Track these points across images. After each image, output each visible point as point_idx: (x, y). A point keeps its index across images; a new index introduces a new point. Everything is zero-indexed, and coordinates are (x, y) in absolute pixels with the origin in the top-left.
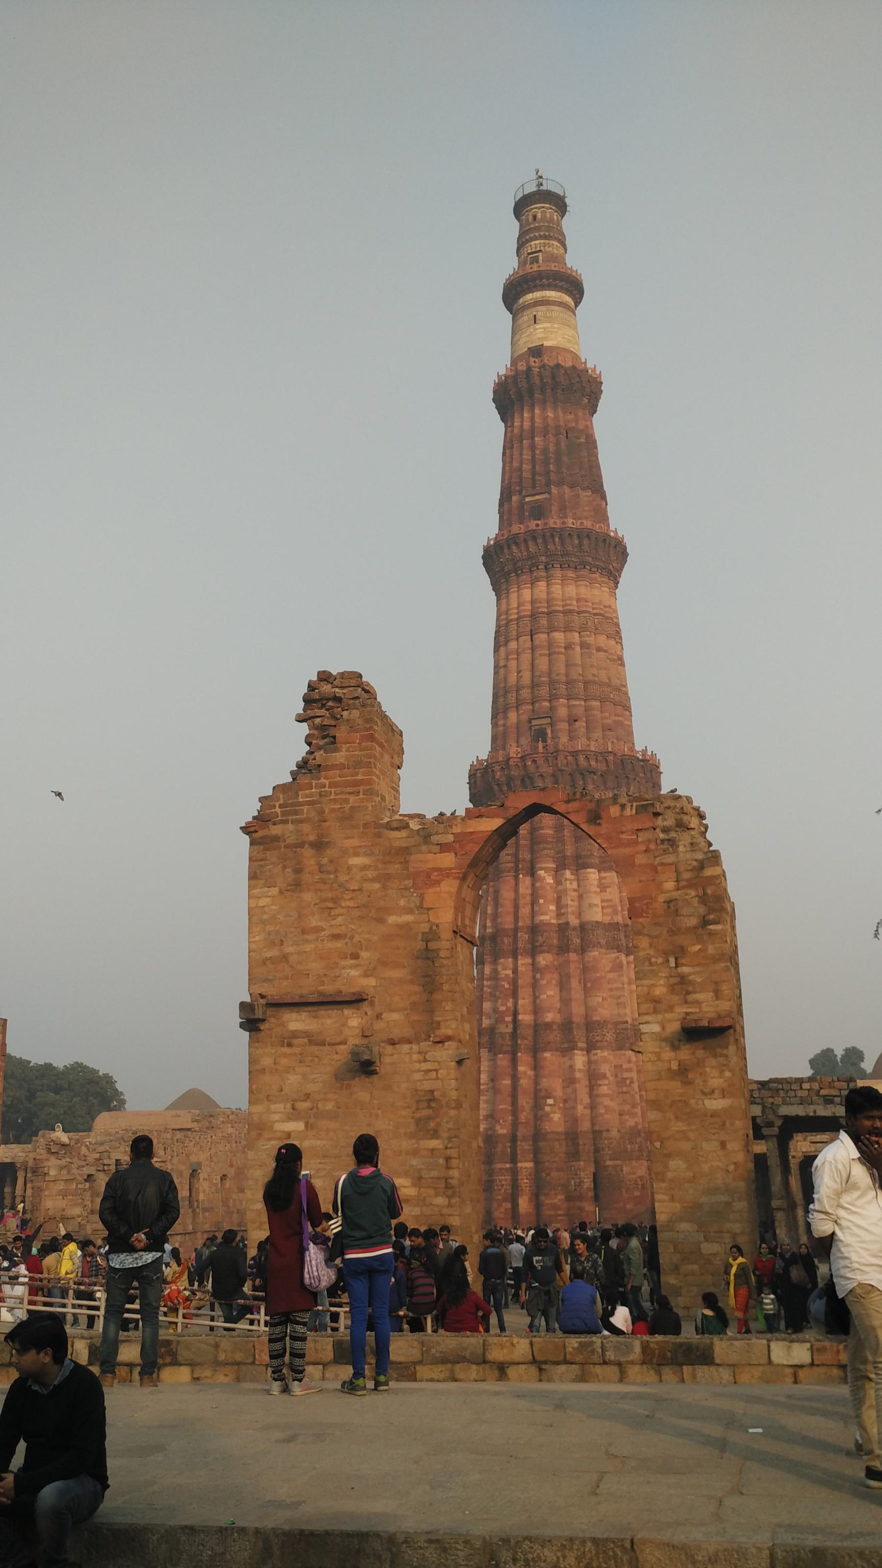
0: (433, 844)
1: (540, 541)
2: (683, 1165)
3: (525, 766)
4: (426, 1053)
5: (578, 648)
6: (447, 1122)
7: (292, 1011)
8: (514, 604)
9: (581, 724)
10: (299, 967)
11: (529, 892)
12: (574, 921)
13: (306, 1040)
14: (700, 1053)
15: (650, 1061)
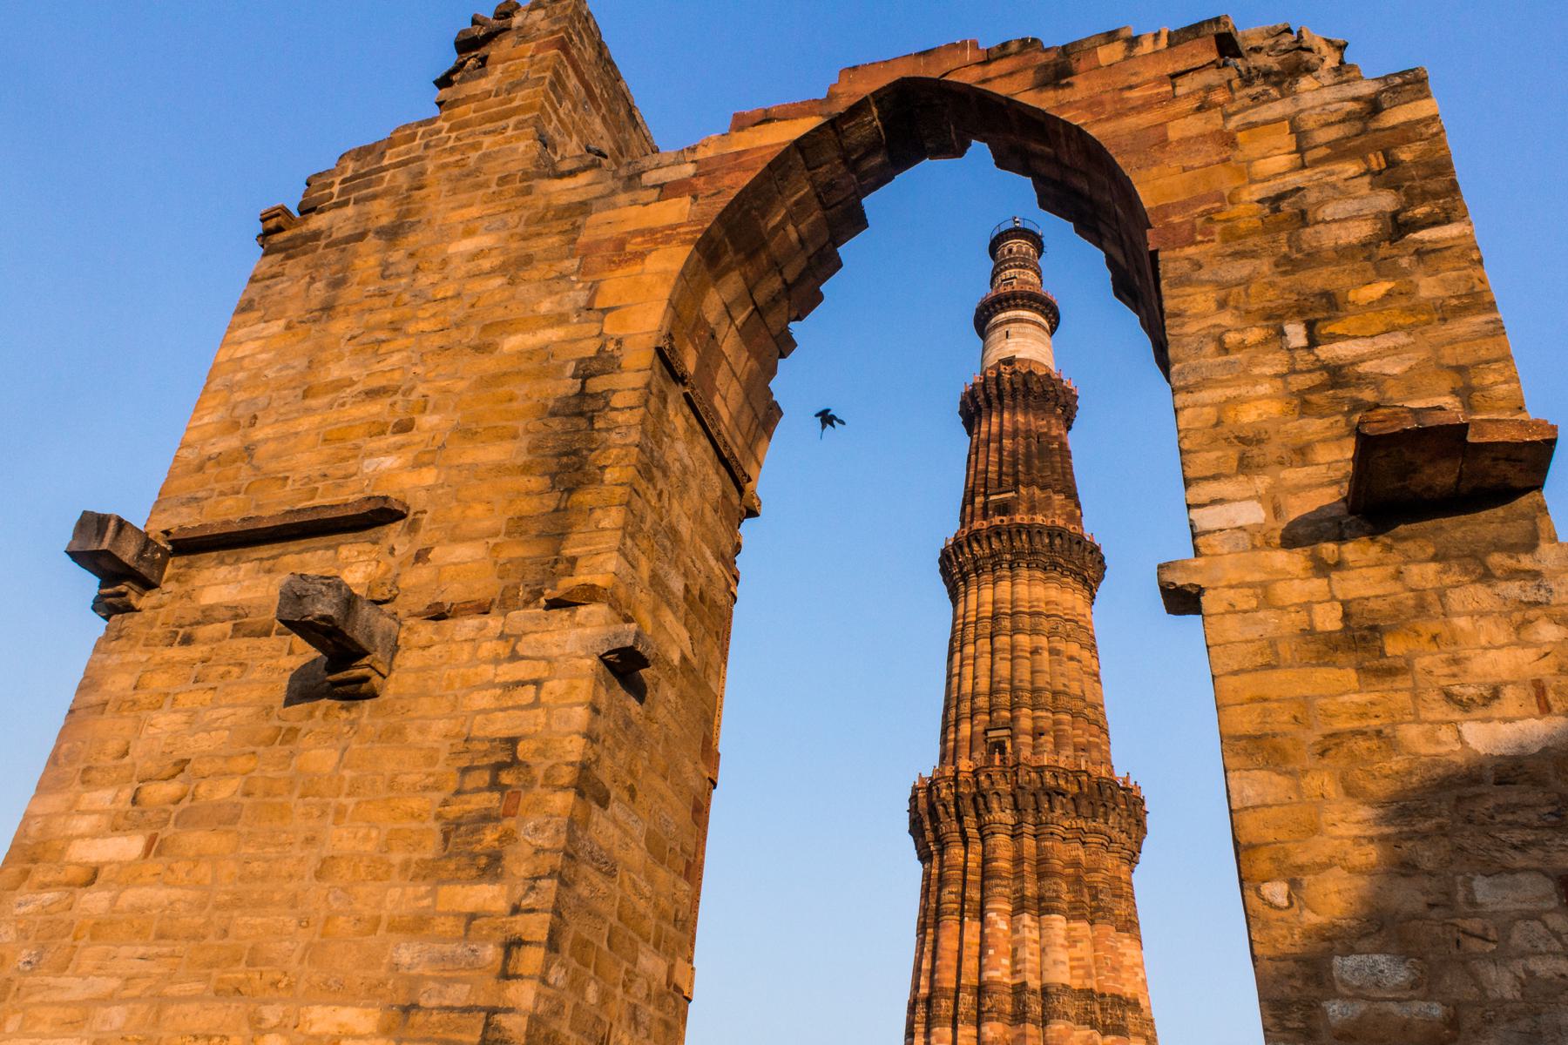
0: (646, 188)
1: (1004, 537)
2: (1394, 972)
3: (977, 782)
4: (519, 638)
5: (1046, 654)
6: (536, 829)
7: (222, 562)
8: (972, 604)
9: (1047, 740)
10: (273, 466)
11: (977, 940)
12: (1034, 983)
13: (228, 626)
14: (1425, 574)
15: (1232, 610)
